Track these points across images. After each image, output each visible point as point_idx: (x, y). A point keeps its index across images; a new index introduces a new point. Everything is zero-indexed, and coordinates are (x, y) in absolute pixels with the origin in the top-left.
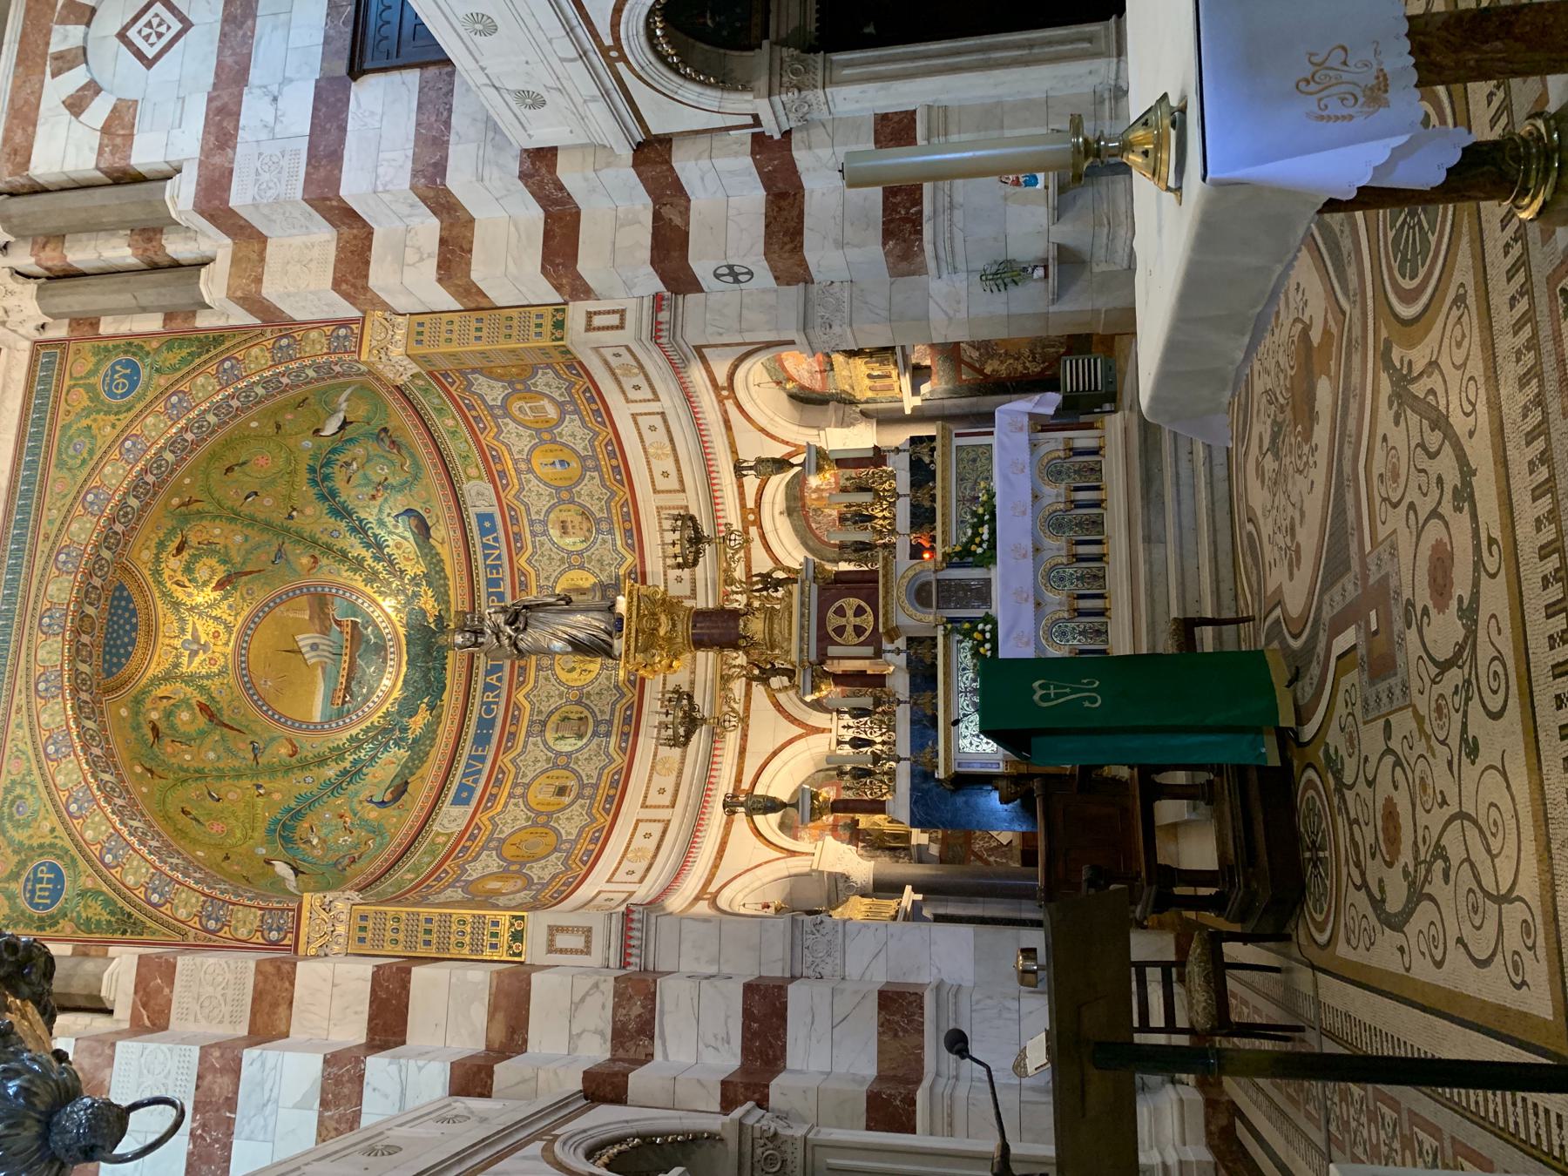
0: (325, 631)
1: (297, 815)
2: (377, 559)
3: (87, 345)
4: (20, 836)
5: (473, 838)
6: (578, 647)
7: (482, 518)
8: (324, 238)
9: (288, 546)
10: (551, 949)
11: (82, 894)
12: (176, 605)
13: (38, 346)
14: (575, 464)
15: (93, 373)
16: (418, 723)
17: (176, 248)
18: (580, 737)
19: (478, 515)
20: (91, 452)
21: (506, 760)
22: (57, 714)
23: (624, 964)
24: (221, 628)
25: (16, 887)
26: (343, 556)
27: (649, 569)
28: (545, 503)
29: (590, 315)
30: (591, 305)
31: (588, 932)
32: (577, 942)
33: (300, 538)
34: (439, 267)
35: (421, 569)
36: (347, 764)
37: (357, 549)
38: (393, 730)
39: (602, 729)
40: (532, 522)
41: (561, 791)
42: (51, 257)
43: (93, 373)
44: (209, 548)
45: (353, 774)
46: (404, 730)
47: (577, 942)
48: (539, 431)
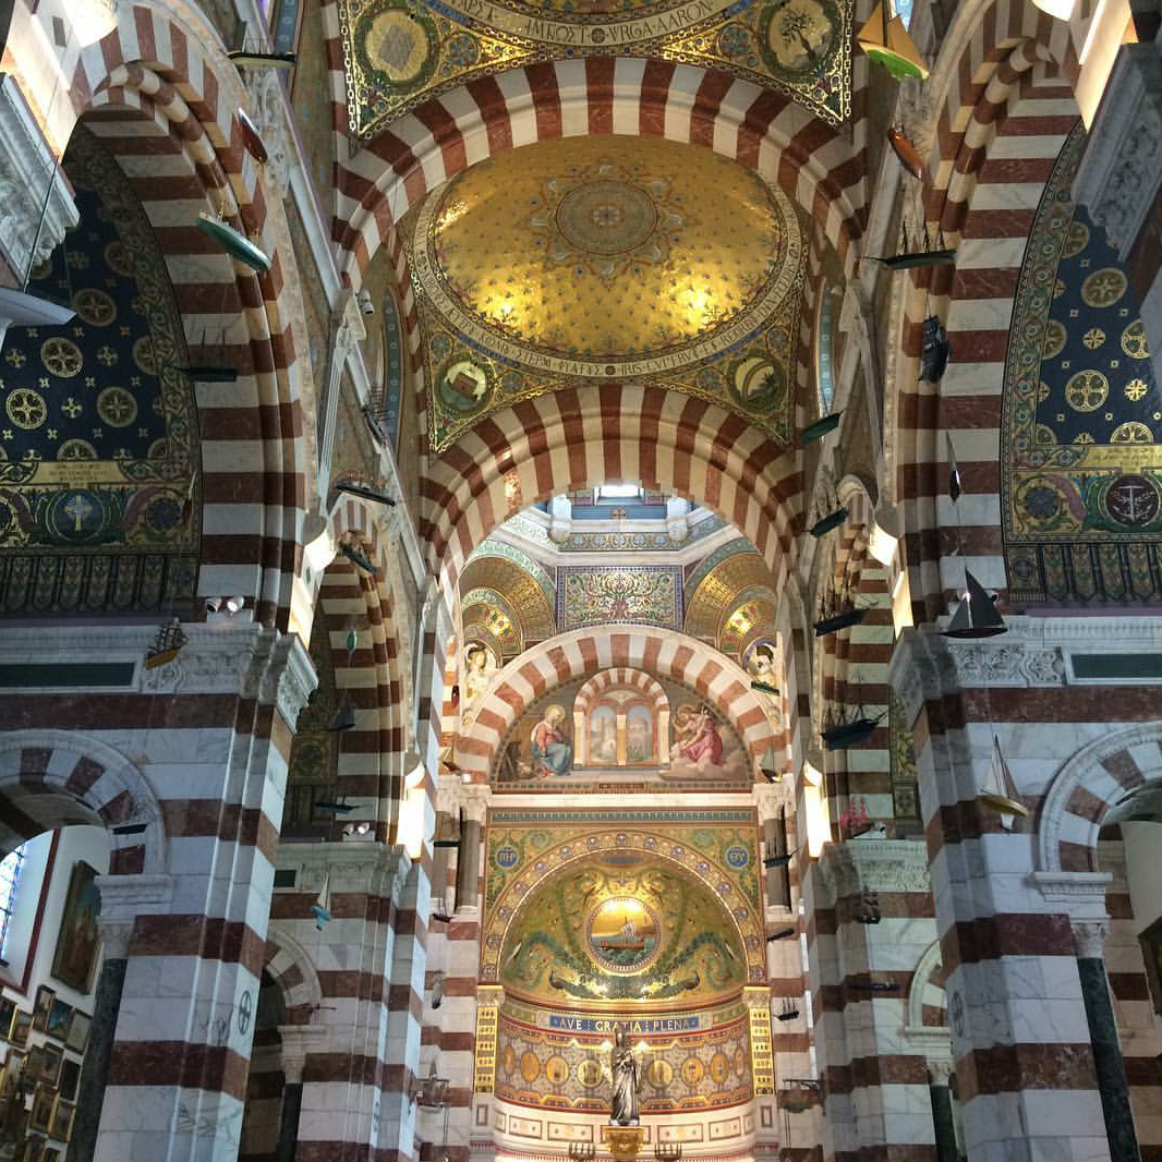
0: (637, 934)
1: (544, 941)
2: (675, 960)
3: (754, 835)
4: (528, 840)
5: (533, 1034)
6: (616, 1099)
7: (697, 1019)
8: (792, 973)
9: (675, 918)
10: (479, 1106)
11: (504, 876)
12: (641, 874)
13: (754, 810)
14: (719, 1078)
15: (741, 841)
16: (592, 986)
17: (793, 890)
18: (586, 1080)
19: (697, 1019)
20: (700, 847)
21: (574, 1041)
22: (580, 849)
23: (472, 1143)
24: (634, 888)
25: (507, 845)
26: (675, 943)
27: (674, 1116)
28: (703, 1058)
29: (769, 1108)
30: (774, 1109)
31: (485, 1124)
32: (481, 1119)
33: (680, 927)
34: (782, 1035)
35: (672, 983)
36: (571, 955)
37: (680, 949)
38: (589, 973)
39: (589, 1092)
40: (694, 1049)
41: (557, 1075)
42: (788, 825)
43: (741, 841)
44: (668, 887)
45: (565, 959)
46: (590, 980)
47: (481, 1119)
48: (733, 1061)
